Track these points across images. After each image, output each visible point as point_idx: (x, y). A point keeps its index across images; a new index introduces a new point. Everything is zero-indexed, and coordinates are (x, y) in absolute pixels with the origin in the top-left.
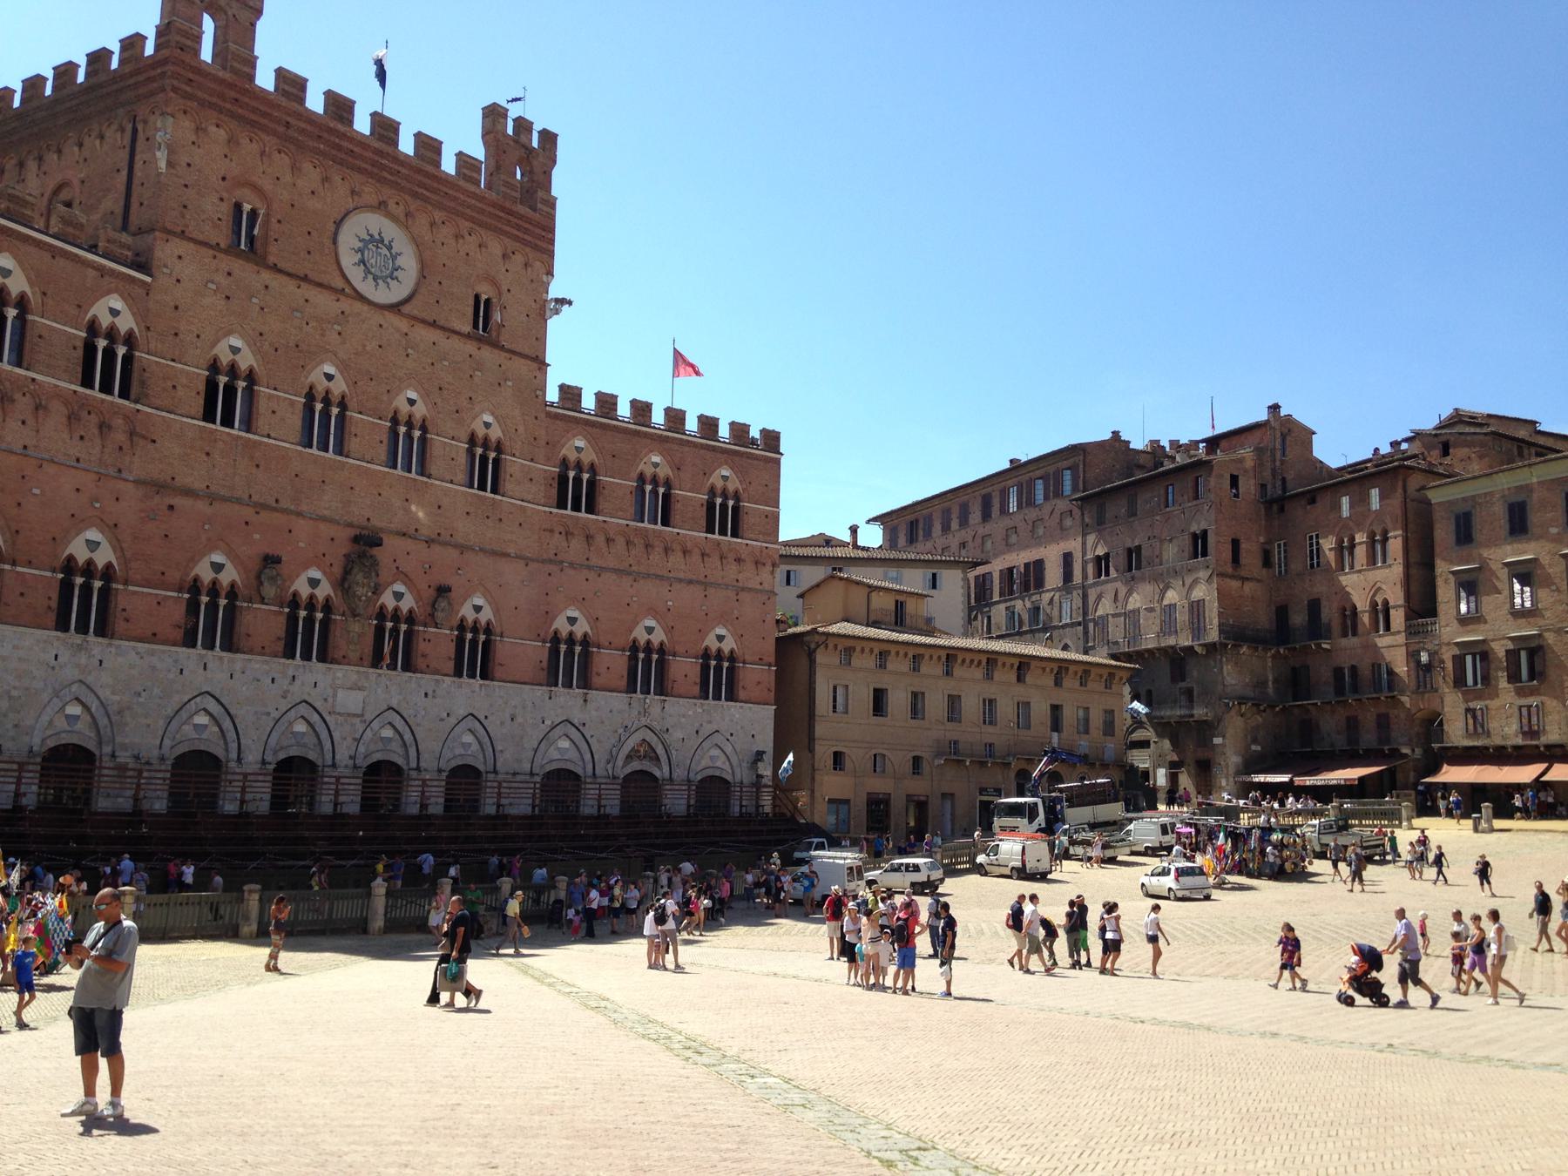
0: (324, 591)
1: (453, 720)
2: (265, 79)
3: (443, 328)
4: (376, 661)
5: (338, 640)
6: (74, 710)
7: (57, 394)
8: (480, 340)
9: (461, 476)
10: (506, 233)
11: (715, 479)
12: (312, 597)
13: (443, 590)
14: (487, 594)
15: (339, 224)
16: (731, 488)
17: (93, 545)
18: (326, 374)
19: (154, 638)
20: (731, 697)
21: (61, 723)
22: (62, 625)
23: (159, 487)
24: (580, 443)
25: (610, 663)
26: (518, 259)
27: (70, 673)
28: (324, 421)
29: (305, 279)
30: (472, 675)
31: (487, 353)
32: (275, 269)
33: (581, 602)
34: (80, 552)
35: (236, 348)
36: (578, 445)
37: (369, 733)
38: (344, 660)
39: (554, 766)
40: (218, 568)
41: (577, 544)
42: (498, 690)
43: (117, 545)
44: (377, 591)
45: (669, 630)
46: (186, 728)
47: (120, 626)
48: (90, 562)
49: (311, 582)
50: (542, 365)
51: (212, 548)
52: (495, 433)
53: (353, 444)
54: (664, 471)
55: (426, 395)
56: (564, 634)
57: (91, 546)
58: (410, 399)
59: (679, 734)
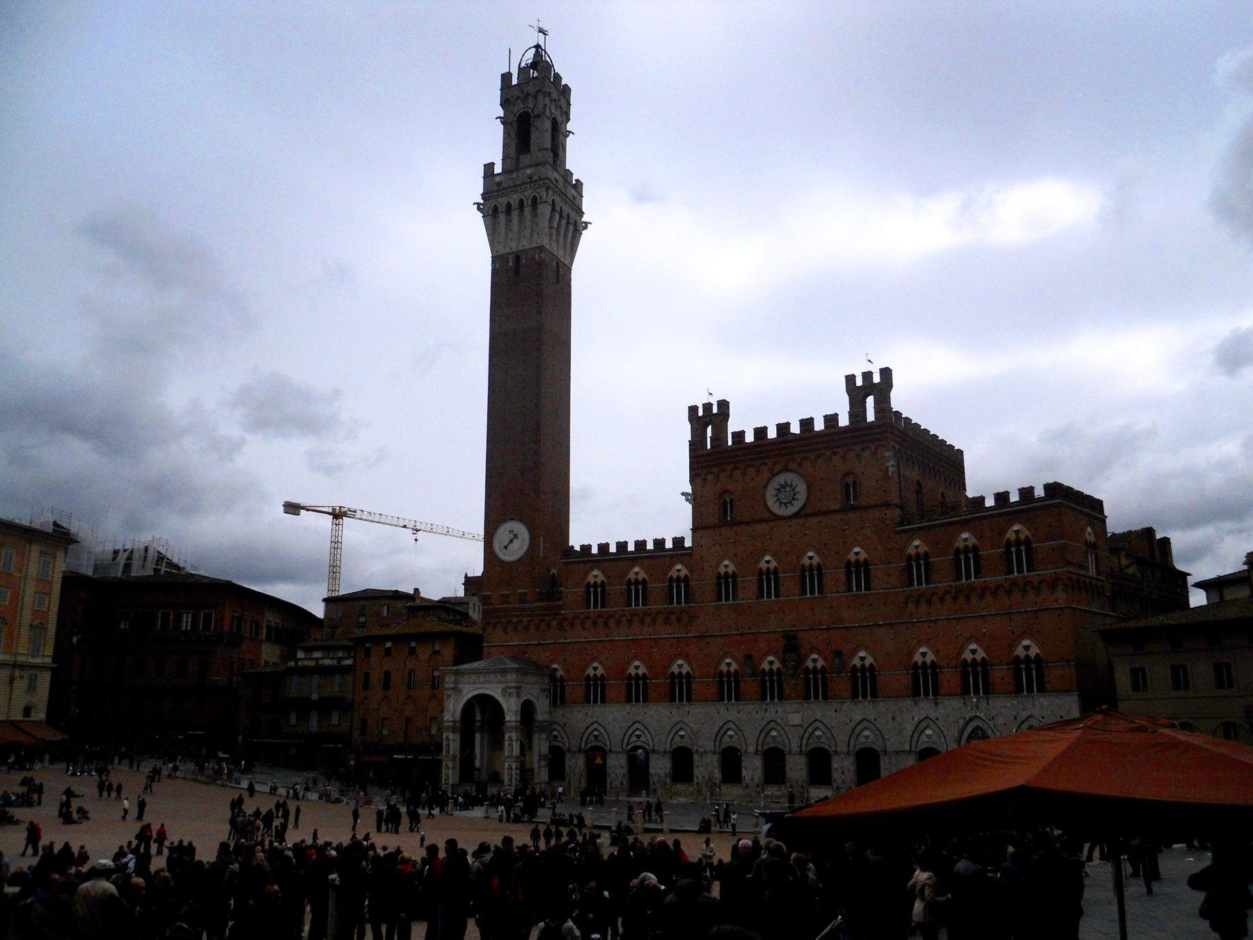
0: (777, 665)
1: (854, 724)
3: (824, 513)
4: (807, 698)
5: (787, 690)
6: (682, 733)
7: (658, 613)
8: (844, 510)
9: (843, 588)
10: (854, 444)
11: (1010, 535)
12: (771, 669)
13: (838, 654)
14: (866, 649)
15: (765, 487)
16: (1022, 537)
17: (680, 666)
18: (768, 561)
19: (706, 700)
20: (1042, 690)
21: (677, 738)
22: (672, 699)
24: (917, 543)
25: (949, 678)
26: (867, 453)
27: (677, 719)
29: (755, 521)
30: (865, 696)
31: (852, 515)
32: (739, 523)
33: (927, 642)
34: (675, 669)
37: (807, 734)
38: (789, 698)
39: (926, 746)
40: (729, 665)
42: (882, 705)
43: (690, 664)
44: (801, 660)
45: (986, 649)
46: (726, 738)
47: (694, 697)
48: (680, 673)
49: (771, 662)
51: (726, 655)
52: (863, 556)
53: (782, 589)
54: (972, 541)
55: (818, 552)
56: (920, 662)
57: (680, 666)
58: (811, 557)
59: (1000, 720)
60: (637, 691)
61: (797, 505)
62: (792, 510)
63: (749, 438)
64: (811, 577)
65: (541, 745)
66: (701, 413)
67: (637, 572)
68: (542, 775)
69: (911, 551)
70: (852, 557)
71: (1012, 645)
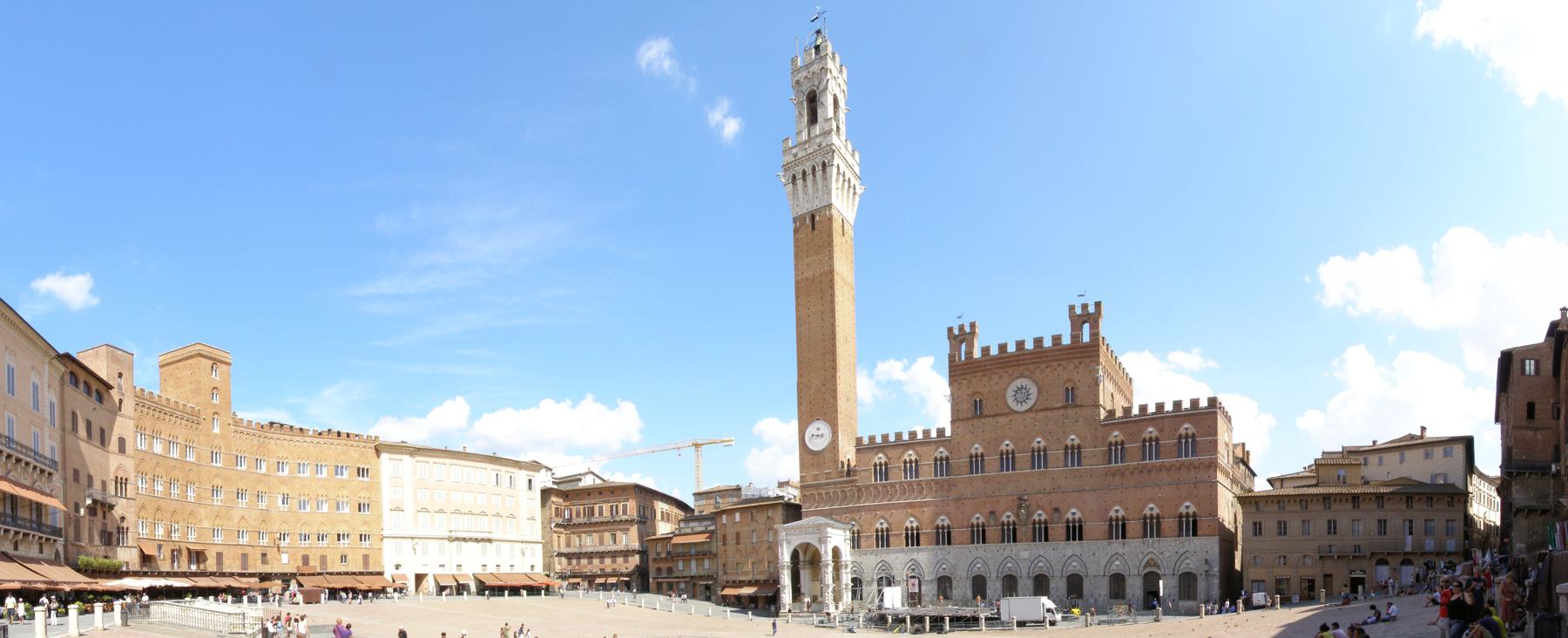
2: (977, 354)
7: (928, 482)
18: (1007, 445)
20: (1195, 534)
23: (958, 500)
28: (1008, 460)
31: (1070, 412)
33: (1120, 503)
35: (977, 448)
36: (1116, 435)
41: (1118, 478)
45: (1161, 507)
50: (1097, 406)
52: (1077, 442)
57: (943, 520)
58: (1039, 442)
60: (913, 539)
61: (1030, 404)
62: (1025, 407)
63: (994, 351)
64: (1040, 458)
65: (846, 578)
66: (956, 332)
67: (911, 455)
68: (847, 597)
69: (1113, 440)
70: (1069, 443)
71: (1178, 506)
